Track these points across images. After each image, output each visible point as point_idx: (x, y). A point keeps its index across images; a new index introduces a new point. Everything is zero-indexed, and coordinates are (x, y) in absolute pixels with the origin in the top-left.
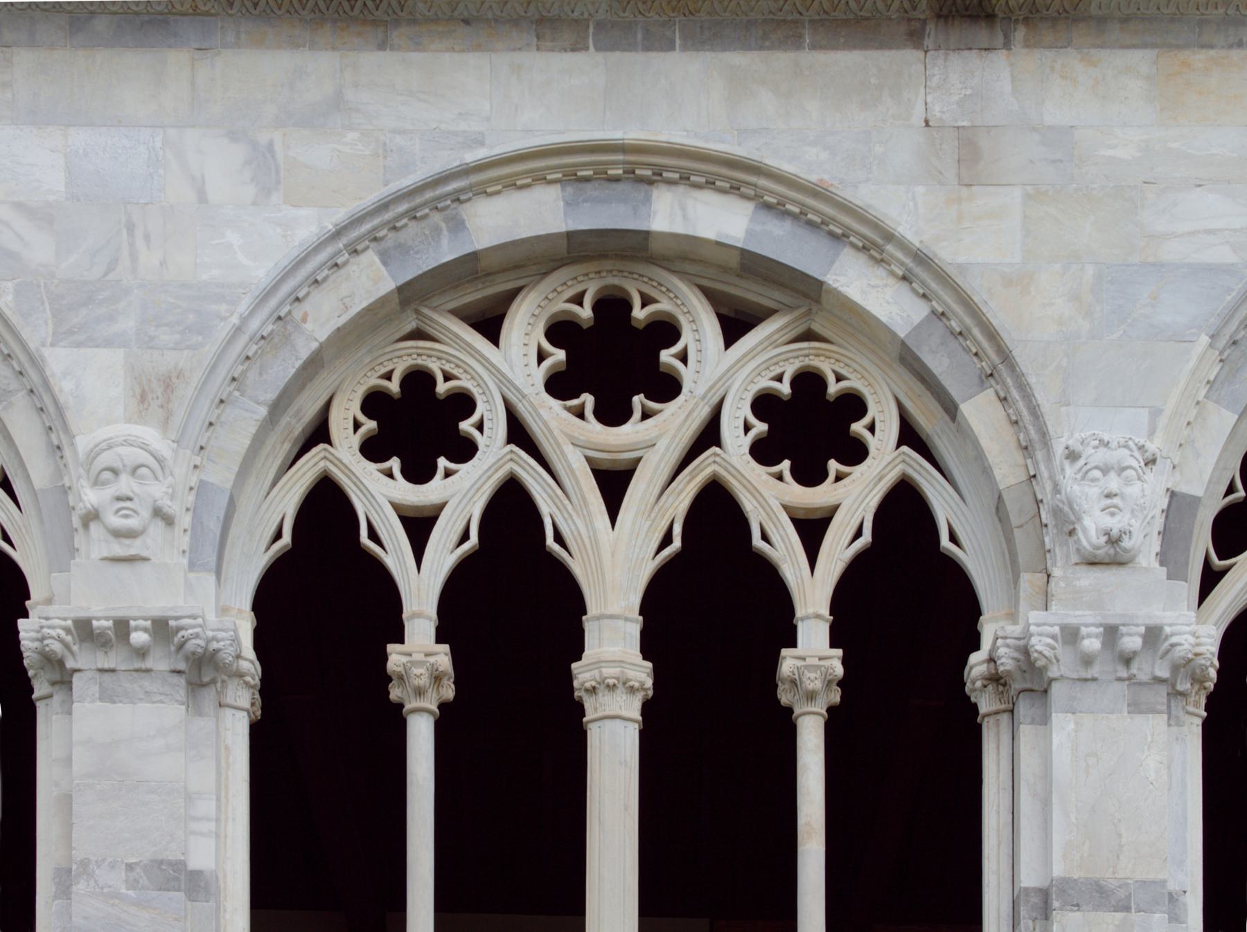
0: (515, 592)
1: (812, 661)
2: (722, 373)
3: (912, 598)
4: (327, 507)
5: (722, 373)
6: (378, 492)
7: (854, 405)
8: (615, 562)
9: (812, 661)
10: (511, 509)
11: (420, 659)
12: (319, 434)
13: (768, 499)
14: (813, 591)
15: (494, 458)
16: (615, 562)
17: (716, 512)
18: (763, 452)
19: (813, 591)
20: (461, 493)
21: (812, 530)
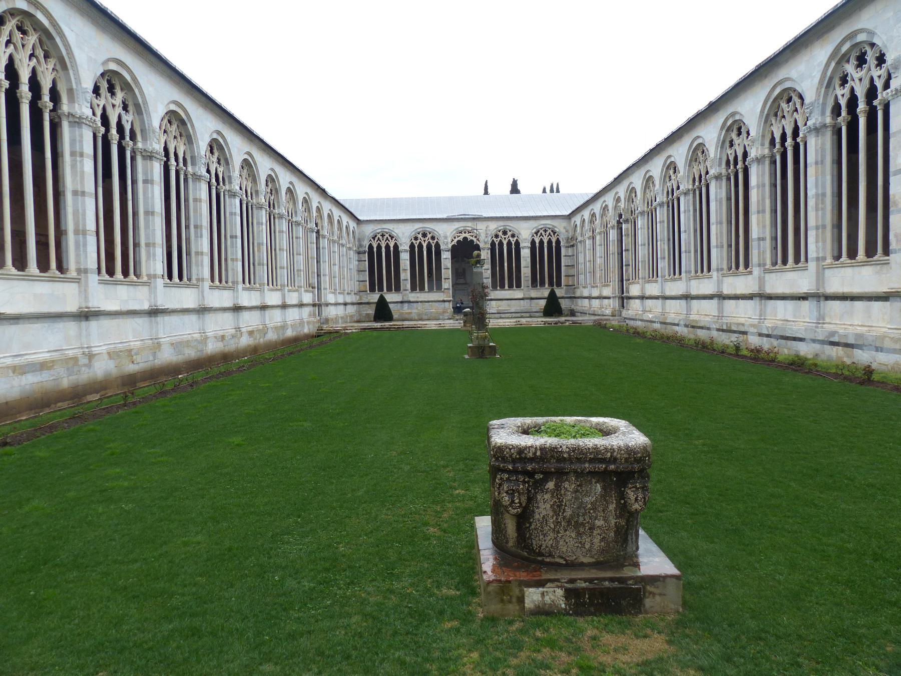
0: (501, 243)
3: (517, 243)
8: (505, 243)
13: (511, 239)
16: (505, 243)
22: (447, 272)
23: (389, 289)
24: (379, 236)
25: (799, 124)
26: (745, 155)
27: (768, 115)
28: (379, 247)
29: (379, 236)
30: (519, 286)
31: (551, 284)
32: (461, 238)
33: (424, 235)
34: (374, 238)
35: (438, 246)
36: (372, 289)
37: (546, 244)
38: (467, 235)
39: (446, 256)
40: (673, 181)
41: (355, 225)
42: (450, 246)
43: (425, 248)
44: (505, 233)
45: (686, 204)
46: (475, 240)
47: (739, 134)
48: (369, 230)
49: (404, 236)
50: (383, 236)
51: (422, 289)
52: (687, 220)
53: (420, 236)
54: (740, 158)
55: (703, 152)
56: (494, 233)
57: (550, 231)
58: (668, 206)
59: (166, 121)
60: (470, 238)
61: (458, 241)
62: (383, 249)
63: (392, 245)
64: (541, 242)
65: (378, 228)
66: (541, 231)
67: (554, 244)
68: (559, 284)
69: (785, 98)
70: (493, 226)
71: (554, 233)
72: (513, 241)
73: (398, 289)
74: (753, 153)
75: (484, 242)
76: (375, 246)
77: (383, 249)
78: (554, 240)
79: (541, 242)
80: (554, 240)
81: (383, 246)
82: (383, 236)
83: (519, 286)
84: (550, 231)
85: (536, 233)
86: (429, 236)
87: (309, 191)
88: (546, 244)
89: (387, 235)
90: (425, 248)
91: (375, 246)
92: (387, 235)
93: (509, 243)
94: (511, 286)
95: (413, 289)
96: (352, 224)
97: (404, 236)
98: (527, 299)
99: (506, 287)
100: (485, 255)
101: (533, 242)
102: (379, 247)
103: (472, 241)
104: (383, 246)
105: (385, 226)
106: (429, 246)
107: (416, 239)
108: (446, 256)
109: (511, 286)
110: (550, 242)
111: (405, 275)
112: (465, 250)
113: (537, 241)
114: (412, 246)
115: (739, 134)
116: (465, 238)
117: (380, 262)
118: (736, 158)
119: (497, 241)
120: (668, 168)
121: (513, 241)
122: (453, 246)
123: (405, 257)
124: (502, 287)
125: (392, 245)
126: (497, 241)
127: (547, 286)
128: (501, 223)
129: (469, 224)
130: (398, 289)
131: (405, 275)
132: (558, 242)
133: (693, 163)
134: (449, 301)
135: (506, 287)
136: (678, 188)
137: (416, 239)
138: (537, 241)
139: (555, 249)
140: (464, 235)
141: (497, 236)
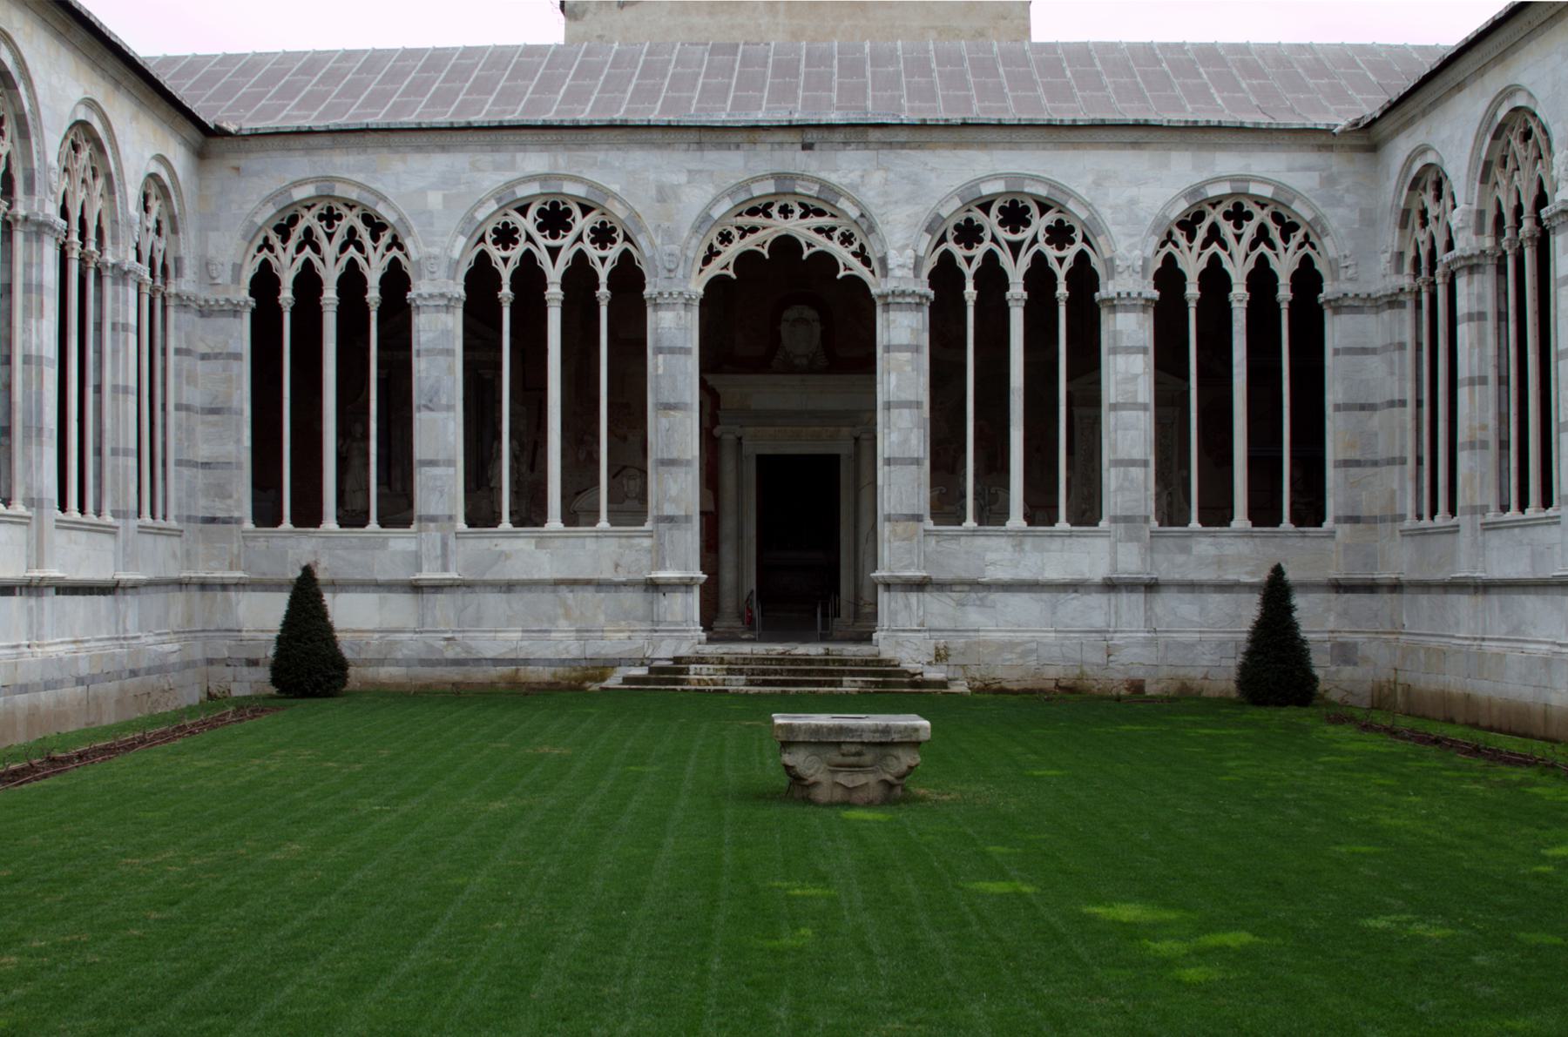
1: (1062, 291)
2: (1039, 224)
3: (1084, 276)
4: (947, 259)
5: (1039, 224)
6: (959, 252)
7: (1072, 229)
8: (1016, 272)
9: (1062, 291)
10: (991, 257)
11: (970, 291)
12: (943, 239)
13: (1051, 253)
14: (1061, 274)
15: (987, 245)
16: (1016, 272)
17: (1039, 258)
18: (1049, 242)
19: (1061, 274)
20: (979, 252)
21: (1061, 260)
22: (675, 432)
23: (352, 517)
24: (309, 219)
25: (1547, 190)
26: (1541, 200)
27: (1487, 165)
28: (308, 282)
29: (309, 219)
30: (1087, 511)
31: (1264, 512)
32: (757, 243)
33: (555, 219)
34: (283, 231)
35: (628, 276)
37: (1239, 293)
38: (798, 227)
39: (674, 329)
40: (1431, 226)
42: (697, 288)
43: (554, 292)
44: (1015, 216)
45: (1474, 294)
46: (843, 254)
47: (1438, 197)
49: (440, 217)
50: (330, 217)
51: (530, 512)
52: (1476, 349)
53: (528, 224)
54: (1509, 220)
55: (1527, 135)
56: (951, 211)
57: (1261, 216)
58: (1418, 305)
59: (68, 143)
62: (330, 295)
63: (373, 276)
64: (1215, 278)
66: (1215, 215)
67: (1284, 293)
68: (1310, 511)
69: (1518, 131)
71: (1288, 229)
72: (1061, 261)
73: (398, 510)
74: (1466, 243)
75: (900, 261)
76: (287, 279)
77: (330, 295)
78: (1284, 265)
79: (1215, 278)
80: (1284, 265)
81: (330, 276)
82: (330, 217)
83: (1087, 511)
84: (1261, 216)
85: (1188, 225)
86: (582, 224)
87: (100, 91)
88: (1239, 293)
89: (351, 219)
90: (554, 292)
91: (287, 279)
92: (351, 219)
93: (1039, 276)
94: (1040, 511)
95: (481, 514)
97: (440, 217)
98: (1131, 586)
99: (1016, 520)
100: (902, 337)
101: (1169, 276)
102: (308, 282)
103: (826, 261)
104: (330, 276)
106: (579, 275)
107: (506, 236)
108: (674, 329)
109: (1040, 511)
110: (1262, 278)
111: (439, 432)
112: (789, 310)
113: (1192, 264)
114: (481, 277)
115: (1438, 197)
116: (785, 245)
117: (320, 378)
118: (1519, 210)
119: (969, 260)
120: (1416, 184)
121: (1061, 261)
122: (716, 286)
123: (438, 335)
124: (992, 512)
125: (373, 276)
126: (969, 260)
127: (1240, 520)
130: (398, 510)
131: (439, 432)
132: (1307, 279)
133: (1496, 171)
134: (685, 585)
135: (1016, 520)
136: (1450, 246)
137: (506, 236)
138: (1192, 264)
139: (1295, 319)
140: (779, 225)
141: (969, 233)
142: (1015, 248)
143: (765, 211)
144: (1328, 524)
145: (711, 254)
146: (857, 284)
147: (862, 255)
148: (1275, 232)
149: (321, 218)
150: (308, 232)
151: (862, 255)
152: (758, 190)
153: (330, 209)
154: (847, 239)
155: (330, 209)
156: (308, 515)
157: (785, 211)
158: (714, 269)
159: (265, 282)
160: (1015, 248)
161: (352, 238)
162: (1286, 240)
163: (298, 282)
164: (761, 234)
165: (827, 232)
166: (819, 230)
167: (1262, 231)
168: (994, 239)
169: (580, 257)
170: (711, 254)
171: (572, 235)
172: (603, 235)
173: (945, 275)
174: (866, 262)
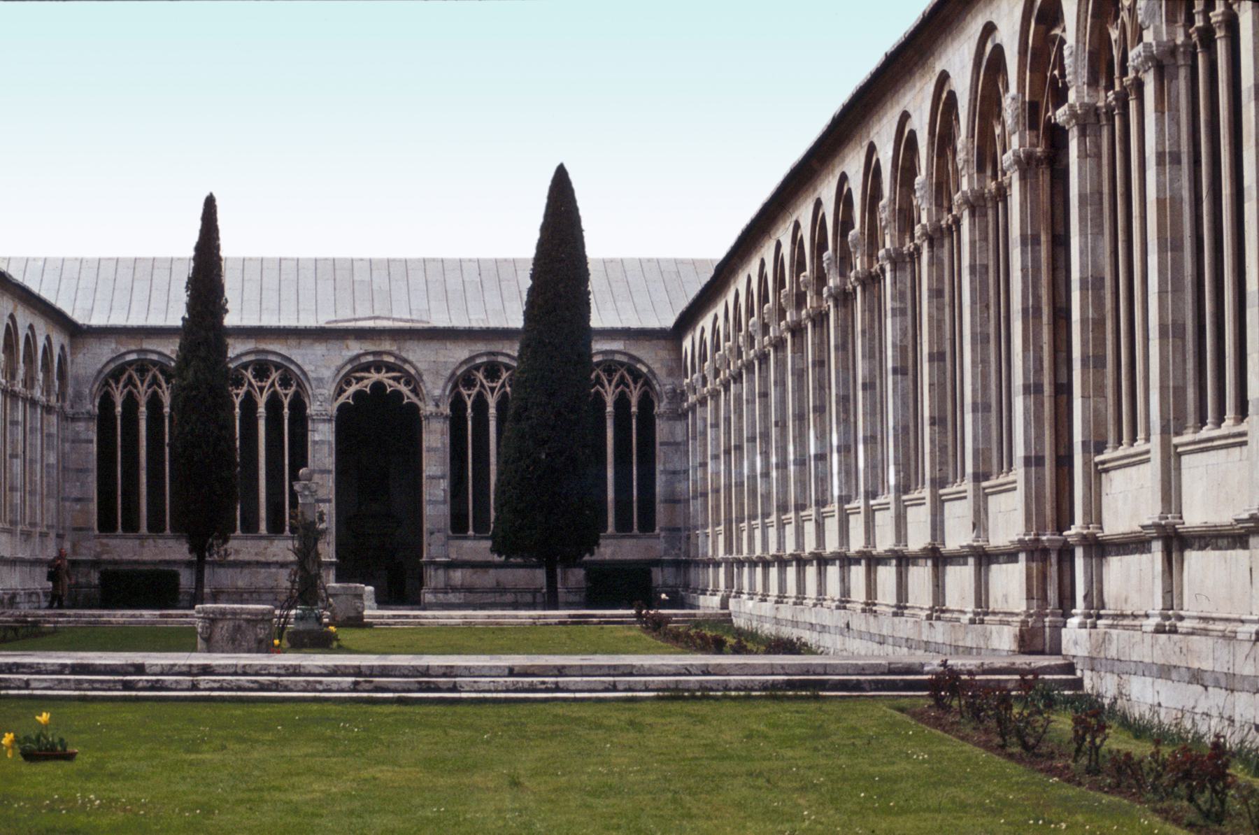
8: (492, 401)
16: (492, 401)
20: (474, 392)
28: (131, 404)
32: (366, 385)
35: (298, 406)
36: (106, 524)
41: (66, 342)
42: (333, 409)
43: (262, 410)
46: (405, 390)
48: (99, 356)
60: (391, 385)
61: (358, 395)
65: (130, 351)
68: (647, 523)
70: (459, 353)
71: (636, 375)
86: (275, 375)
90: (262, 410)
96: (58, 339)
102: (131, 404)
103: (398, 395)
105: (148, 345)
106: (274, 404)
116: (378, 386)
122: (343, 408)
128: (481, 347)
129: (387, 346)
132: (647, 403)
141: (468, 381)
142: (492, 390)
143: (366, 368)
144: (657, 531)
145: (340, 391)
146: (414, 409)
147: (415, 391)
148: (629, 378)
149: (137, 371)
150: (130, 377)
151: (415, 391)
152: (364, 360)
153: (142, 365)
154: (407, 383)
155: (142, 365)
156: (131, 526)
157: (378, 370)
158: (342, 399)
159: (106, 403)
160: (492, 390)
161: (155, 381)
162: (635, 382)
163: (125, 404)
164: (366, 382)
165: (397, 379)
166: (394, 379)
167: (622, 381)
168: (482, 385)
169: (275, 393)
170: (340, 391)
171: (270, 381)
172: (285, 383)
173: (458, 404)
174: (417, 395)
